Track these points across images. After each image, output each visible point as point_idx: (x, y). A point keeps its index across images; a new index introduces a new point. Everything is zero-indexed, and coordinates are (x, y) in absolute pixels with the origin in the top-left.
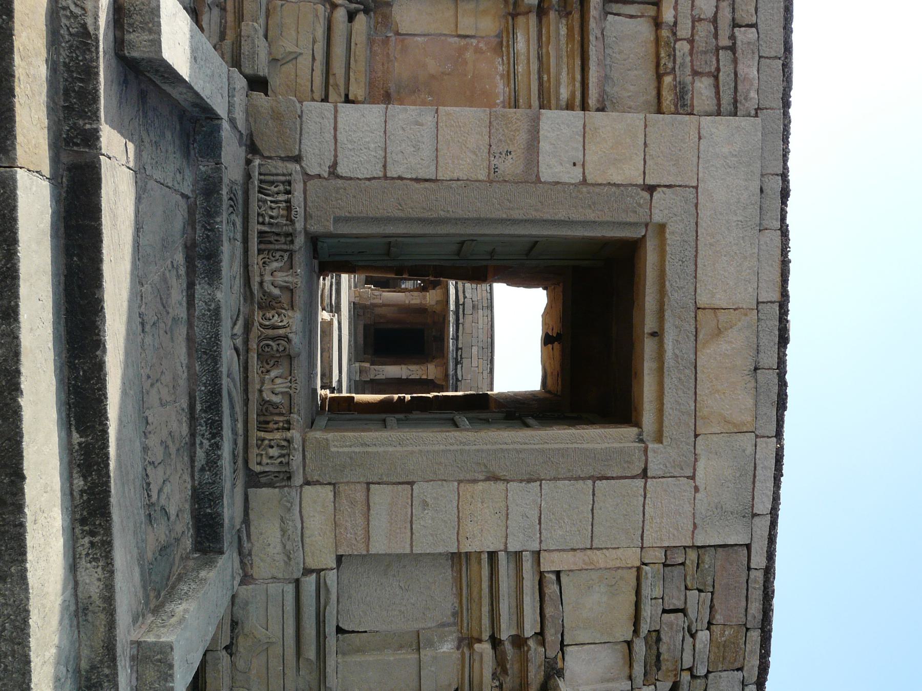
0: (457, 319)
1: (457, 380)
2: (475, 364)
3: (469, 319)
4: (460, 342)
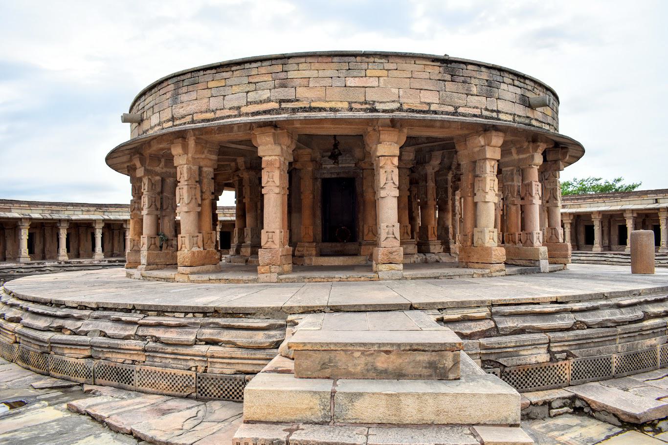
0: (304, 110)
1: (400, 109)
2: (373, 82)
3: (302, 93)
4: (339, 105)
